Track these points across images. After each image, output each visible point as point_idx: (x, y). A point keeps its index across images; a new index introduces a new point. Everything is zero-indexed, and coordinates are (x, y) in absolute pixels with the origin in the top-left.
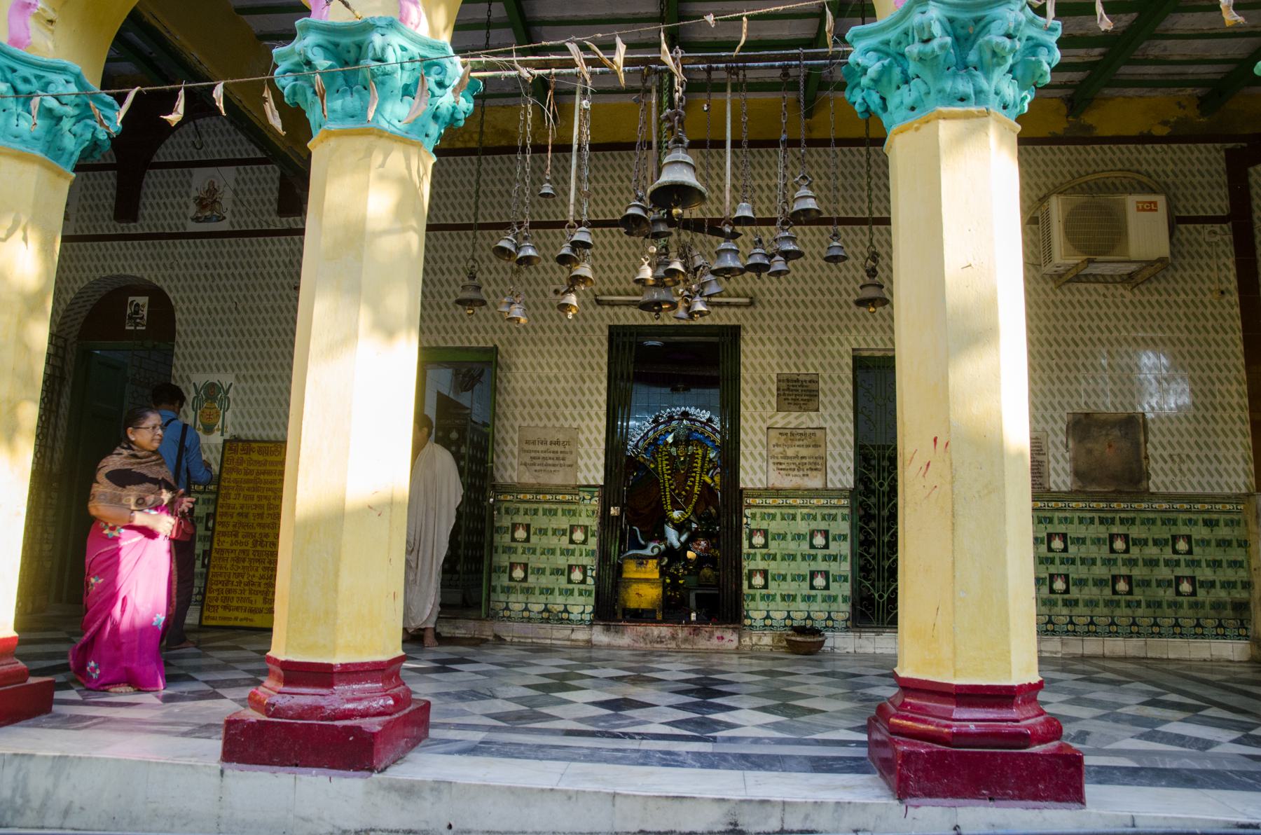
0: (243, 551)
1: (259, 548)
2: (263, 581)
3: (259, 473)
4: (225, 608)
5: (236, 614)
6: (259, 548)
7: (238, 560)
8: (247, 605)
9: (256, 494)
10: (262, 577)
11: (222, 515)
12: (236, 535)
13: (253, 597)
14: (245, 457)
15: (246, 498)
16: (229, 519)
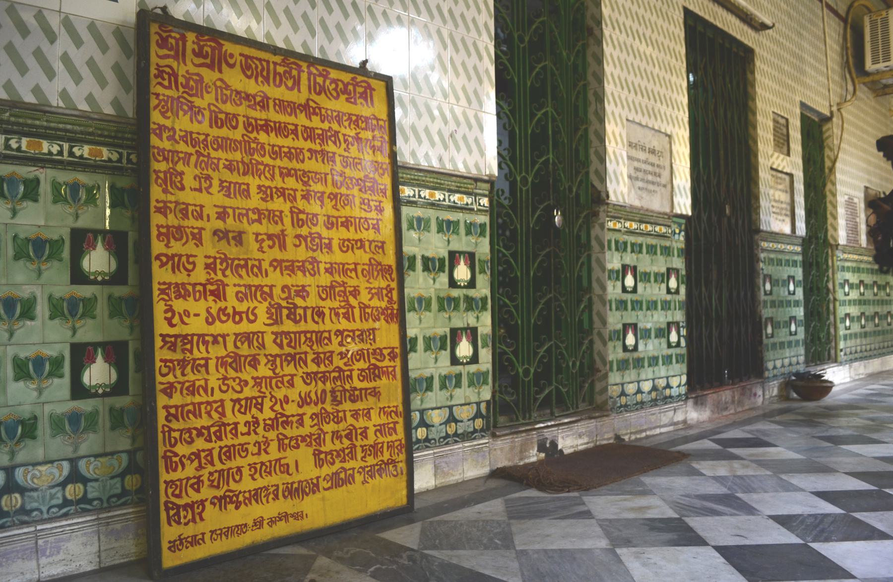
0: (248, 337)
1: (288, 326)
2: (309, 410)
3: (252, 126)
4: (222, 502)
5: (257, 510)
6: (288, 326)
7: (236, 362)
8: (276, 479)
9: (254, 182)
10: (304, 401)
11: (168, 234)
12: (219, 294)
13: (290, 456)
14: (209, 76)
15: (227, 189)
16: (190, 248)
